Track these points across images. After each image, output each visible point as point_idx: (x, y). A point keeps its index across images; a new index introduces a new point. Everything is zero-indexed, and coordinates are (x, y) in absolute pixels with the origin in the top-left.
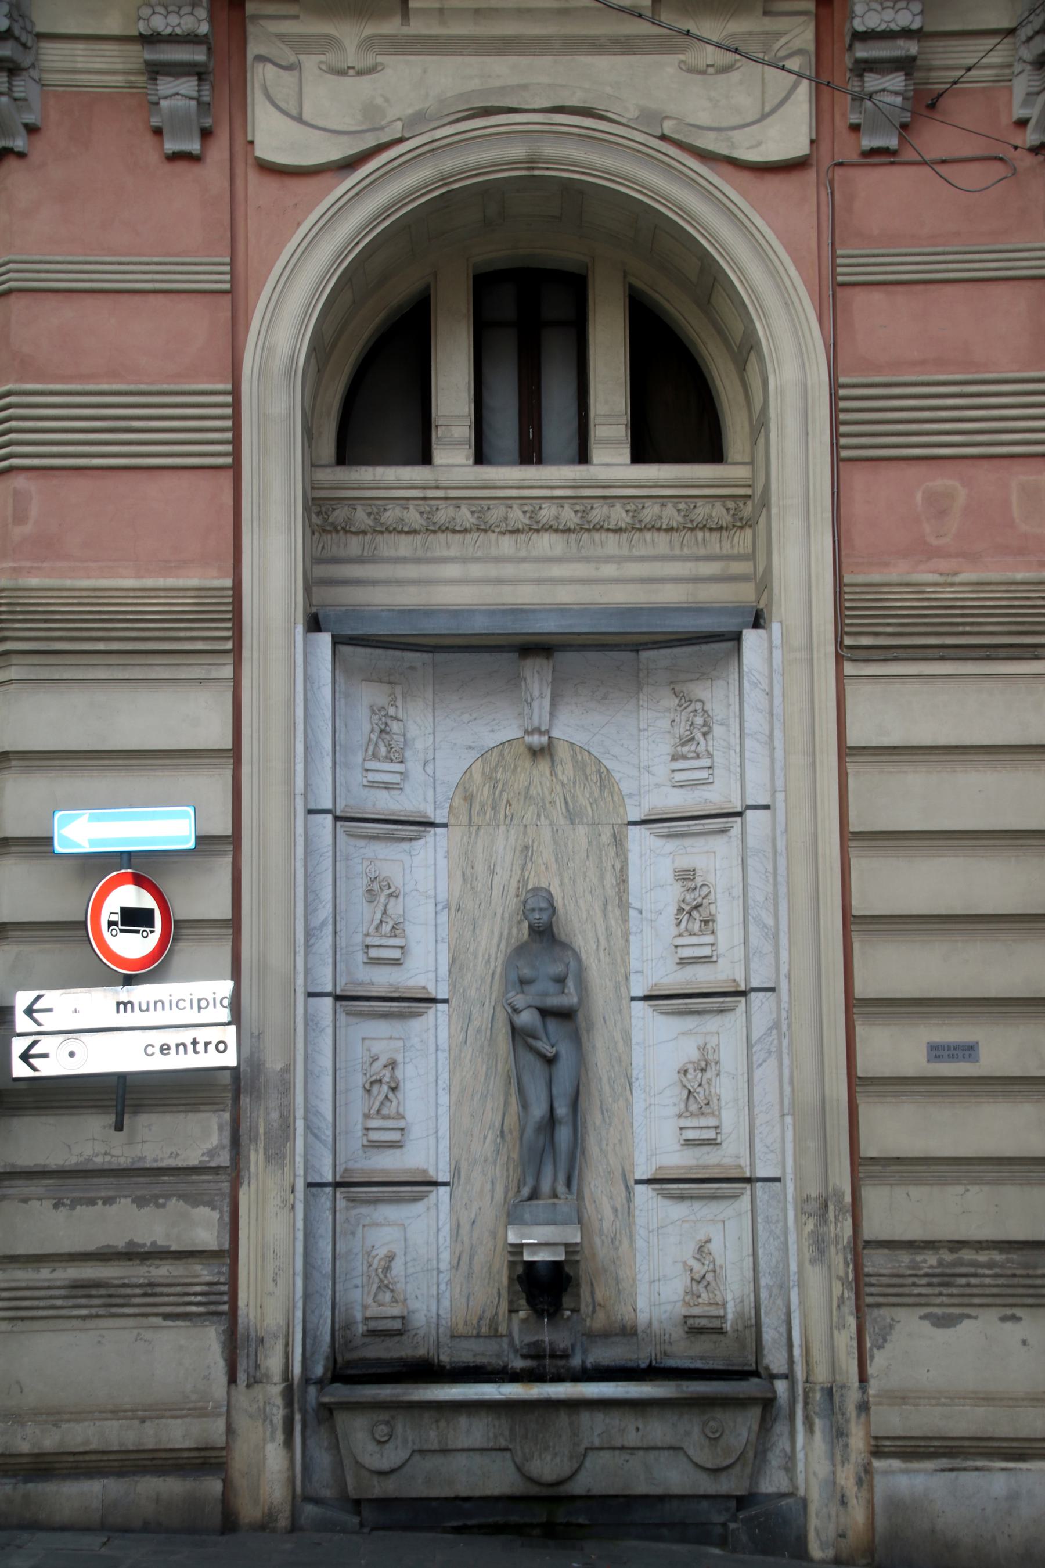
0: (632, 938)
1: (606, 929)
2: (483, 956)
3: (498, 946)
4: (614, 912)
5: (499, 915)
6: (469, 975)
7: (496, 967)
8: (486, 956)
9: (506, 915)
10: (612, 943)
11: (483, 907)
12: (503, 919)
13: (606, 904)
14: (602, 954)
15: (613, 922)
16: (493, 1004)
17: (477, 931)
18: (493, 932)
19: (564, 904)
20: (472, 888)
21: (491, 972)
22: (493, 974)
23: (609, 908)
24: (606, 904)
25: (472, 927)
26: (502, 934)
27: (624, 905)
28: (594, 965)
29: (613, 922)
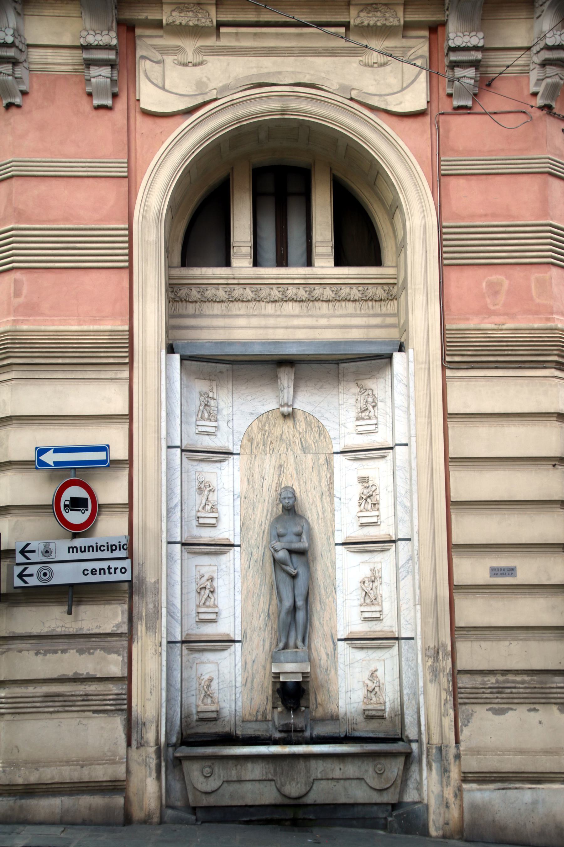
0: (336, 513)
2: (258, 522)
3: (266, 517)
4: (326, 500)
6: (251, 532)
9: (270, 501)
12: (268, 503)
13: (322, 495)
14: (320, 521)
15: (326, 505)
16: (264, 547)
18: (263, 510)
21: (262, 530)
22: (264, 532)
24: (322, 495)
27: (331, 495)
28: (316, 527)
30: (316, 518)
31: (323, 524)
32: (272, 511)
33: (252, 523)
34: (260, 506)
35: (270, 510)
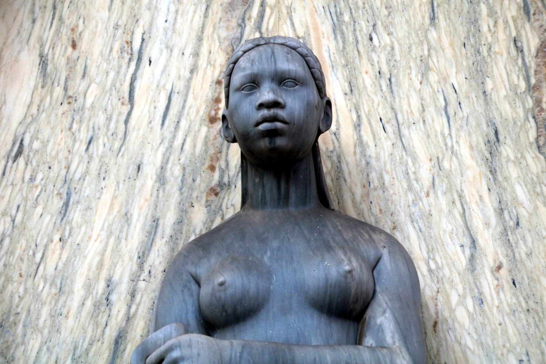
1: (500, 211)
2: (89, 287)
3: (142, 258)
5: (150, 172)
7: (129, 319)
8: (101, 286)
9: (175, 172)
10: (522, 250)
11: (98, 148)
12: (161, 180)
13: (495, 139)
14: (488, 283)
15: (521, 193)
17: (76, 215)
18: (127, 217)
19: (360, 142)
20: (70, 99)
21: (111, 333)
23: (507, 150)
24: (495, 139)
25: (57, 204)
26: (156, 221)
28: (461, 315)
29: (521, 193)
30: (462, 261)
31: (508, 296)
32: (180, 222)
33: (47, 292)
34: (107, 197)
35: (169, 219)
